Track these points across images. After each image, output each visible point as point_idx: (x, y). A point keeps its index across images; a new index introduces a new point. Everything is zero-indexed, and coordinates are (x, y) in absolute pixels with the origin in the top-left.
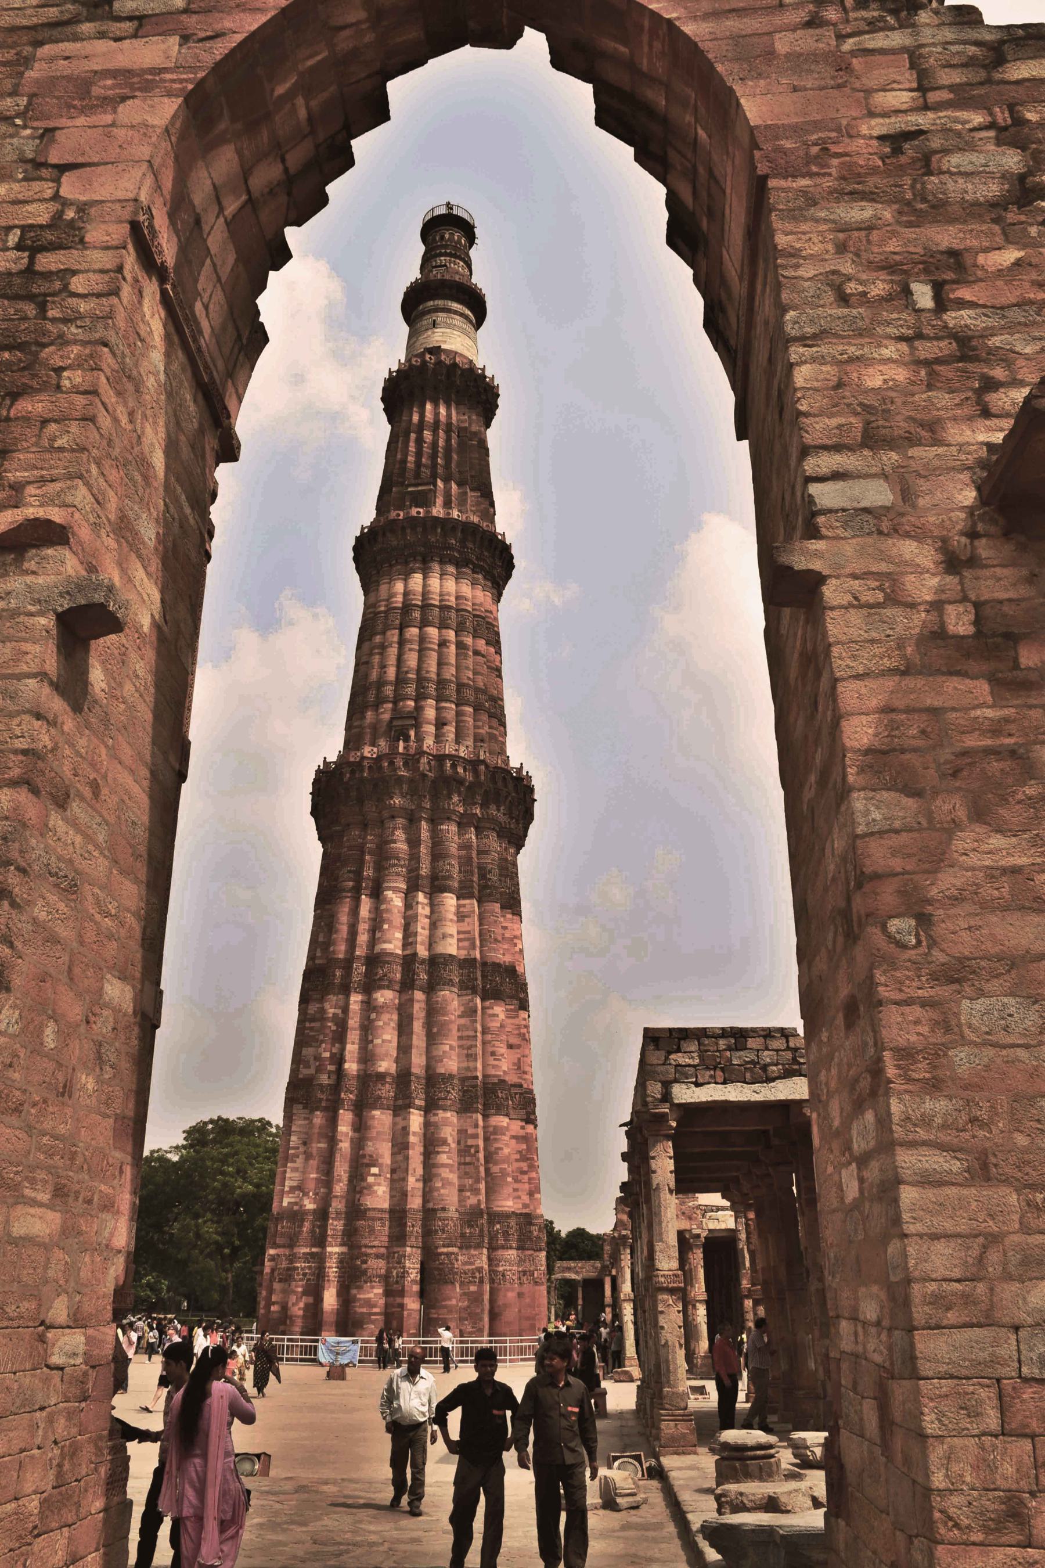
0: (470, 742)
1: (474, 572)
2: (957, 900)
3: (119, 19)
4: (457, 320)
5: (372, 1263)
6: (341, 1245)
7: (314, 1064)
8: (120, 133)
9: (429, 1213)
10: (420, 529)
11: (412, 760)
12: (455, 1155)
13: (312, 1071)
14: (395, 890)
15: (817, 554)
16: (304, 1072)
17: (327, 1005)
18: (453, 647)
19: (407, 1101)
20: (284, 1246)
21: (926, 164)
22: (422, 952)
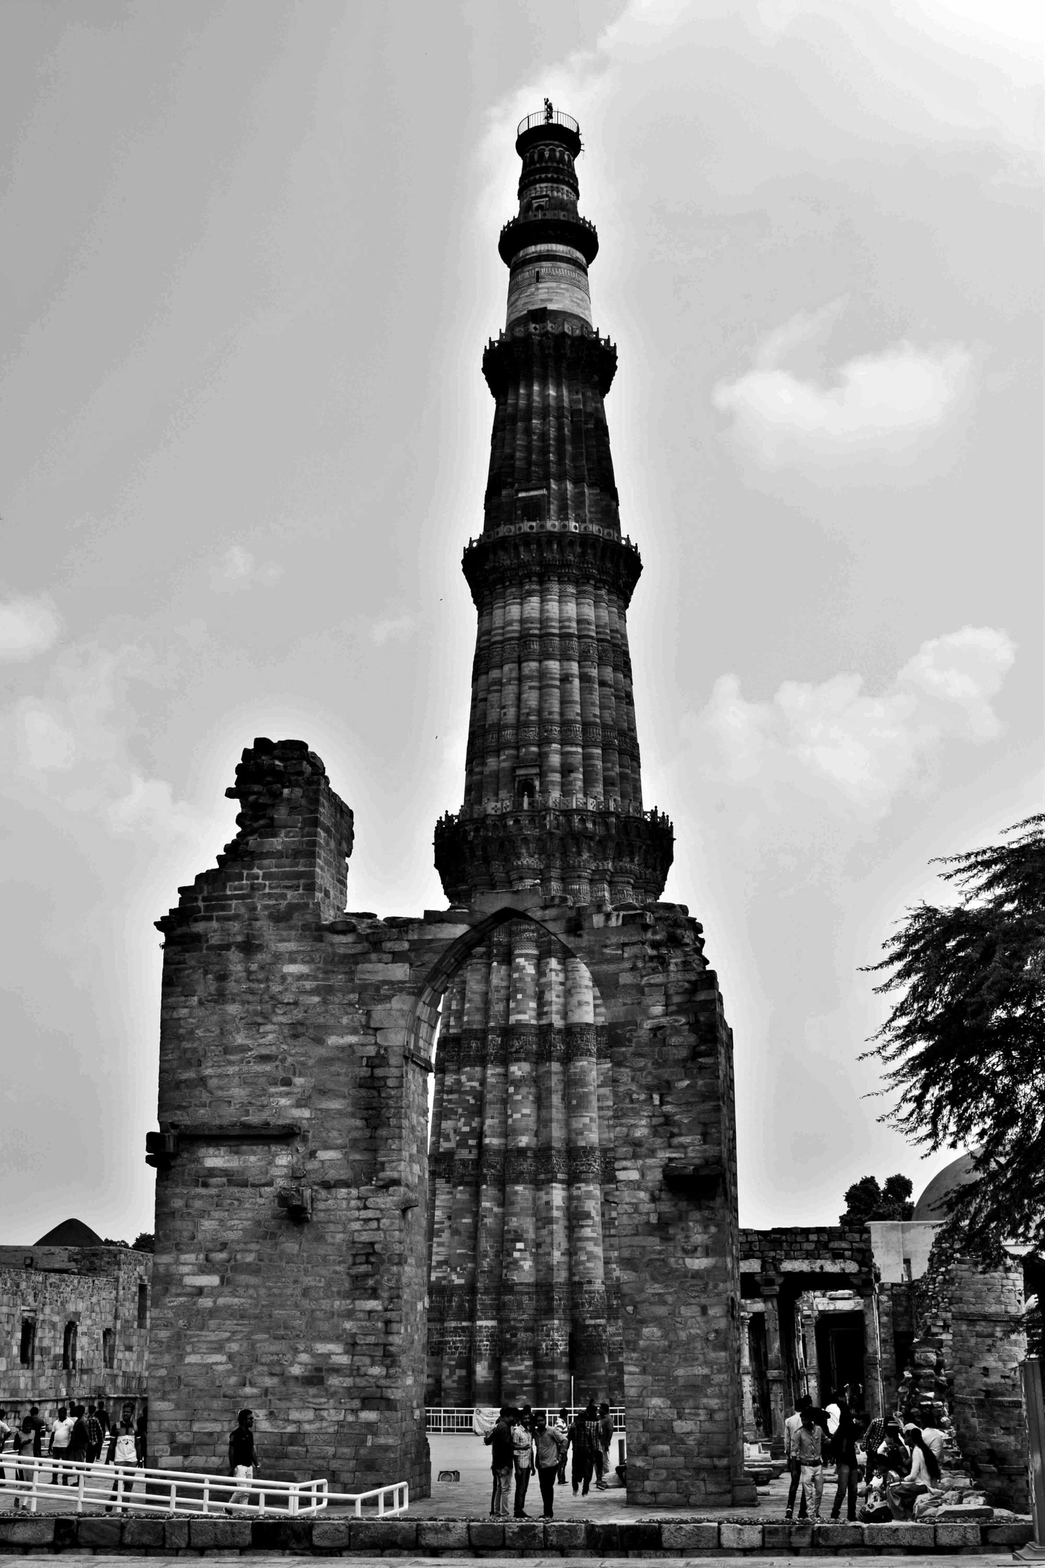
0: (599, 788)
1: (597, 588)
2: (643, 1302)
3: (385, 952)
4: (564, 269)
5: (521, 1335)
6: (492, 1319)
7: (455, 1139)
8: (393, 1013)
9: (576, 1286)
10: (534, 547)
11: (538, 813)
12: (599, 1230)
13: (452, 1145)
14: (526, 956)
15: (616, 1196)
16: (444, 1146)
17: (464, 1078)
18: (576, 682)
19: (549, 1176)
21: (664, 1042)
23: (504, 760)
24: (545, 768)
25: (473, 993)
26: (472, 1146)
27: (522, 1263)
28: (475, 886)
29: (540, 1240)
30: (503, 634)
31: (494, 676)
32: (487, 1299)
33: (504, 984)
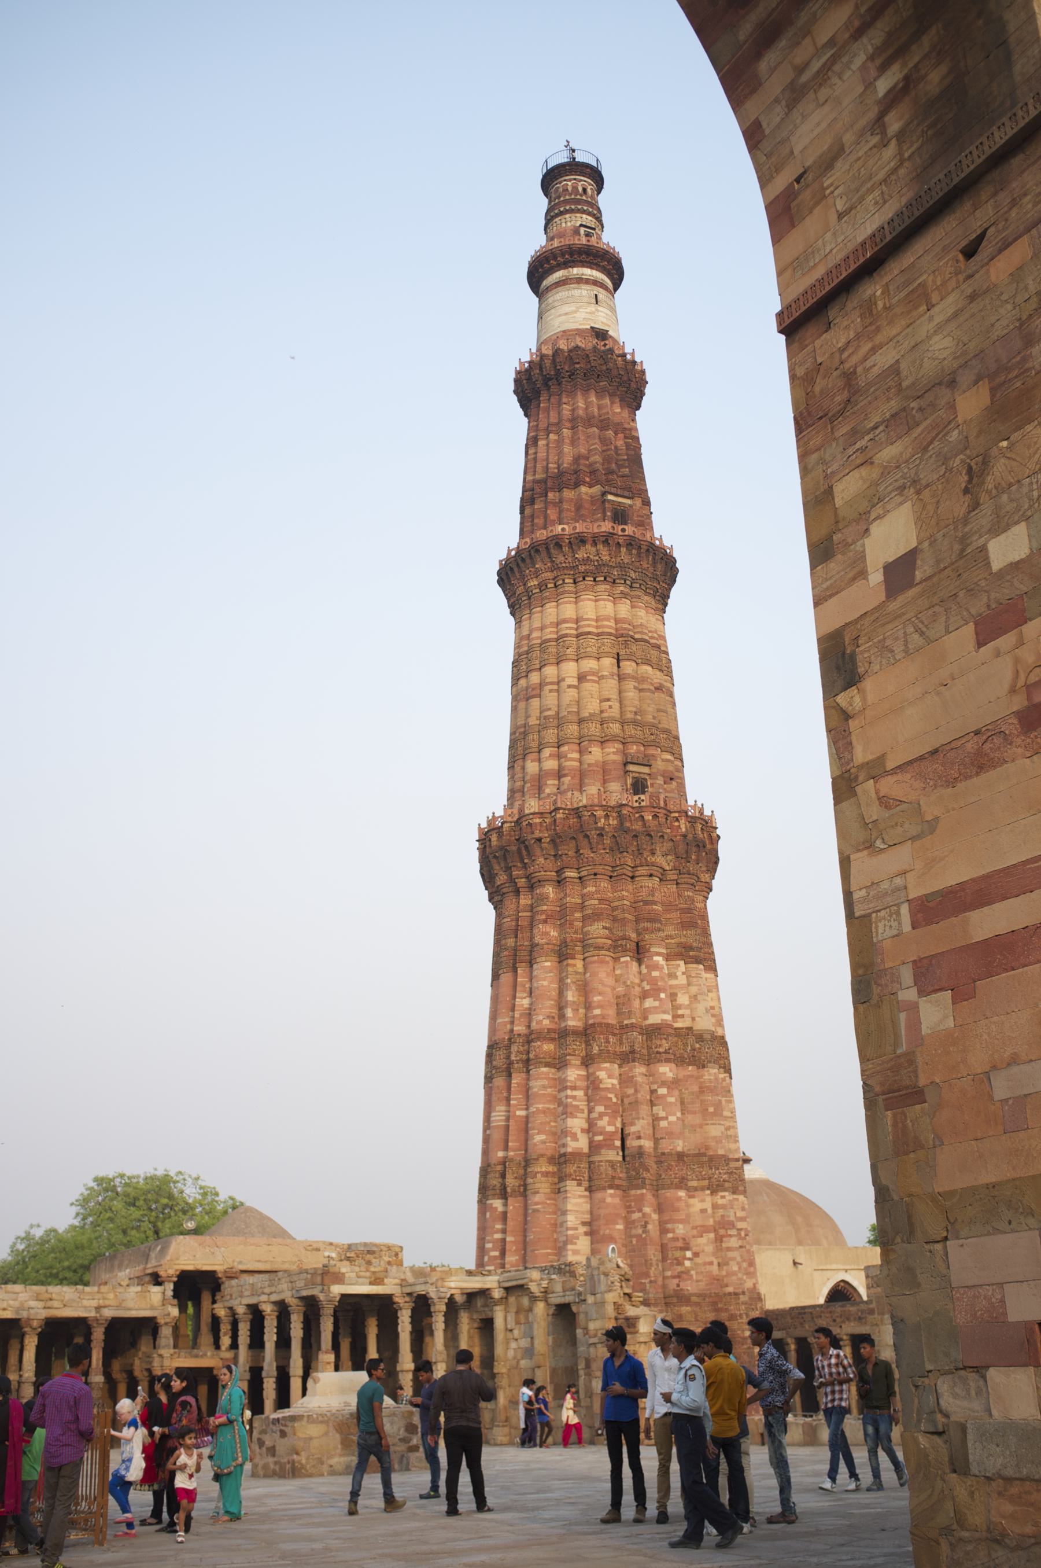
10: (634, 552)
16: (572, 1146)
17: (602, 1075)
23: (614, 753)
25: (603, 985)
28: (595, 874)
31: (591, 666)
33: (637, 981)
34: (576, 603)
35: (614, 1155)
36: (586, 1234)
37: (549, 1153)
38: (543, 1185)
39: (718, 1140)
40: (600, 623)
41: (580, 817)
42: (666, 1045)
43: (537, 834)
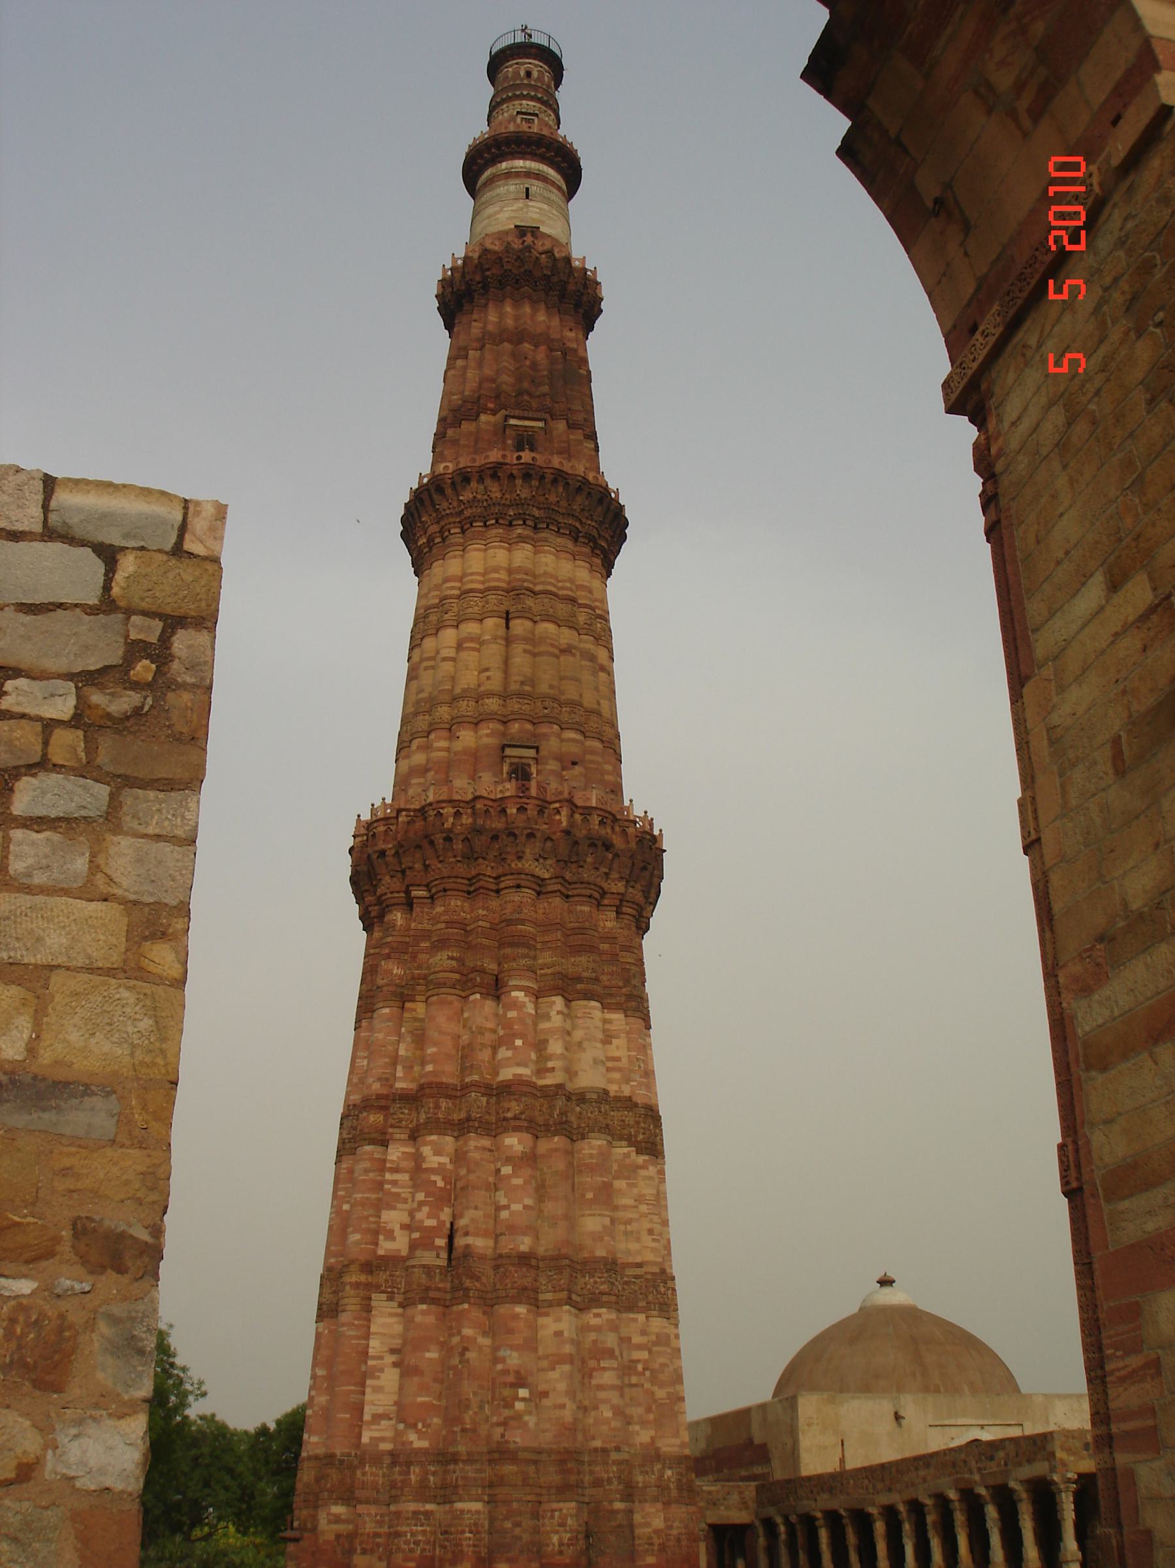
4: (555, 196)
6: (478, 1499)
10: (535, 483)
13: (399, 1244)
16: (385, 1247)
17: (426, 1151)
20: (367, 1502)
22: (570, 1087)
24: (543, 753)
25: (441, 1033)
26: (440, 1247)
27: (526, 1418)
28: (445, 890)
29: (542, 1387)
30: (483, 583)
31: (469, 630)
32: (470, 1471)
33: (490, 1025)
34: (462, 556)
35: (434, 1258)
36: (395, 1365)
37: (363, 1258)
38: (354, 1301)
39: (597, 1237)
40: (487, 577)
41: (425, 819)
42: (515, 1107)
43: (381, 846)
